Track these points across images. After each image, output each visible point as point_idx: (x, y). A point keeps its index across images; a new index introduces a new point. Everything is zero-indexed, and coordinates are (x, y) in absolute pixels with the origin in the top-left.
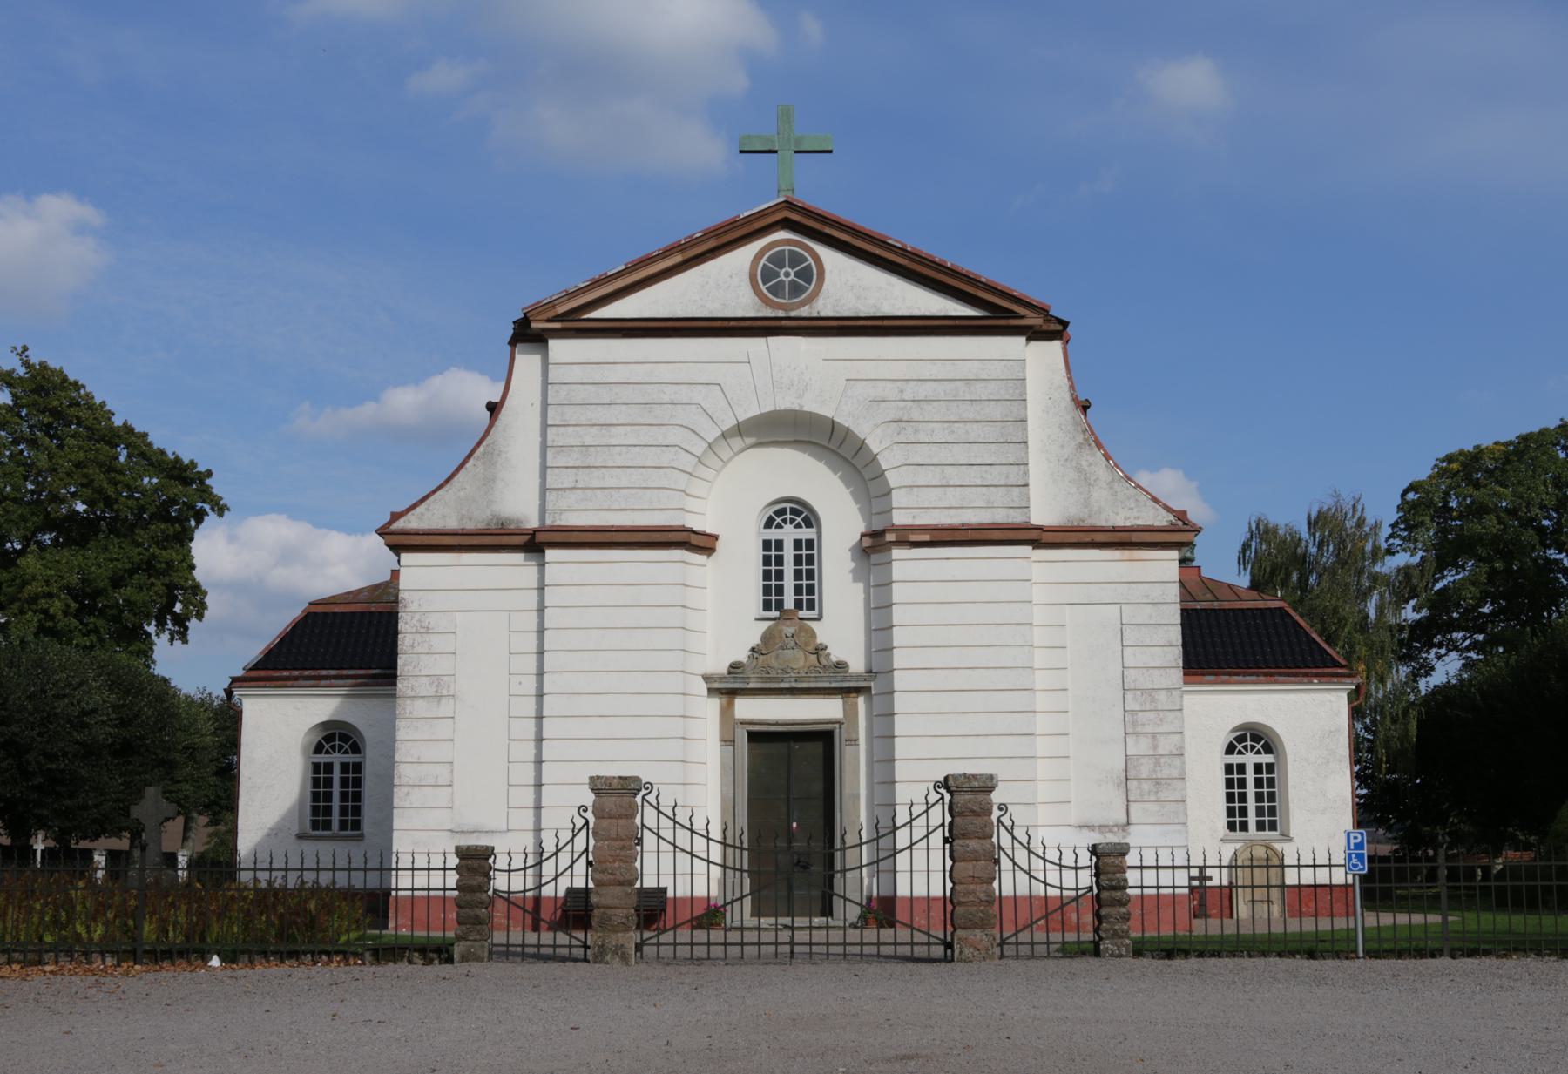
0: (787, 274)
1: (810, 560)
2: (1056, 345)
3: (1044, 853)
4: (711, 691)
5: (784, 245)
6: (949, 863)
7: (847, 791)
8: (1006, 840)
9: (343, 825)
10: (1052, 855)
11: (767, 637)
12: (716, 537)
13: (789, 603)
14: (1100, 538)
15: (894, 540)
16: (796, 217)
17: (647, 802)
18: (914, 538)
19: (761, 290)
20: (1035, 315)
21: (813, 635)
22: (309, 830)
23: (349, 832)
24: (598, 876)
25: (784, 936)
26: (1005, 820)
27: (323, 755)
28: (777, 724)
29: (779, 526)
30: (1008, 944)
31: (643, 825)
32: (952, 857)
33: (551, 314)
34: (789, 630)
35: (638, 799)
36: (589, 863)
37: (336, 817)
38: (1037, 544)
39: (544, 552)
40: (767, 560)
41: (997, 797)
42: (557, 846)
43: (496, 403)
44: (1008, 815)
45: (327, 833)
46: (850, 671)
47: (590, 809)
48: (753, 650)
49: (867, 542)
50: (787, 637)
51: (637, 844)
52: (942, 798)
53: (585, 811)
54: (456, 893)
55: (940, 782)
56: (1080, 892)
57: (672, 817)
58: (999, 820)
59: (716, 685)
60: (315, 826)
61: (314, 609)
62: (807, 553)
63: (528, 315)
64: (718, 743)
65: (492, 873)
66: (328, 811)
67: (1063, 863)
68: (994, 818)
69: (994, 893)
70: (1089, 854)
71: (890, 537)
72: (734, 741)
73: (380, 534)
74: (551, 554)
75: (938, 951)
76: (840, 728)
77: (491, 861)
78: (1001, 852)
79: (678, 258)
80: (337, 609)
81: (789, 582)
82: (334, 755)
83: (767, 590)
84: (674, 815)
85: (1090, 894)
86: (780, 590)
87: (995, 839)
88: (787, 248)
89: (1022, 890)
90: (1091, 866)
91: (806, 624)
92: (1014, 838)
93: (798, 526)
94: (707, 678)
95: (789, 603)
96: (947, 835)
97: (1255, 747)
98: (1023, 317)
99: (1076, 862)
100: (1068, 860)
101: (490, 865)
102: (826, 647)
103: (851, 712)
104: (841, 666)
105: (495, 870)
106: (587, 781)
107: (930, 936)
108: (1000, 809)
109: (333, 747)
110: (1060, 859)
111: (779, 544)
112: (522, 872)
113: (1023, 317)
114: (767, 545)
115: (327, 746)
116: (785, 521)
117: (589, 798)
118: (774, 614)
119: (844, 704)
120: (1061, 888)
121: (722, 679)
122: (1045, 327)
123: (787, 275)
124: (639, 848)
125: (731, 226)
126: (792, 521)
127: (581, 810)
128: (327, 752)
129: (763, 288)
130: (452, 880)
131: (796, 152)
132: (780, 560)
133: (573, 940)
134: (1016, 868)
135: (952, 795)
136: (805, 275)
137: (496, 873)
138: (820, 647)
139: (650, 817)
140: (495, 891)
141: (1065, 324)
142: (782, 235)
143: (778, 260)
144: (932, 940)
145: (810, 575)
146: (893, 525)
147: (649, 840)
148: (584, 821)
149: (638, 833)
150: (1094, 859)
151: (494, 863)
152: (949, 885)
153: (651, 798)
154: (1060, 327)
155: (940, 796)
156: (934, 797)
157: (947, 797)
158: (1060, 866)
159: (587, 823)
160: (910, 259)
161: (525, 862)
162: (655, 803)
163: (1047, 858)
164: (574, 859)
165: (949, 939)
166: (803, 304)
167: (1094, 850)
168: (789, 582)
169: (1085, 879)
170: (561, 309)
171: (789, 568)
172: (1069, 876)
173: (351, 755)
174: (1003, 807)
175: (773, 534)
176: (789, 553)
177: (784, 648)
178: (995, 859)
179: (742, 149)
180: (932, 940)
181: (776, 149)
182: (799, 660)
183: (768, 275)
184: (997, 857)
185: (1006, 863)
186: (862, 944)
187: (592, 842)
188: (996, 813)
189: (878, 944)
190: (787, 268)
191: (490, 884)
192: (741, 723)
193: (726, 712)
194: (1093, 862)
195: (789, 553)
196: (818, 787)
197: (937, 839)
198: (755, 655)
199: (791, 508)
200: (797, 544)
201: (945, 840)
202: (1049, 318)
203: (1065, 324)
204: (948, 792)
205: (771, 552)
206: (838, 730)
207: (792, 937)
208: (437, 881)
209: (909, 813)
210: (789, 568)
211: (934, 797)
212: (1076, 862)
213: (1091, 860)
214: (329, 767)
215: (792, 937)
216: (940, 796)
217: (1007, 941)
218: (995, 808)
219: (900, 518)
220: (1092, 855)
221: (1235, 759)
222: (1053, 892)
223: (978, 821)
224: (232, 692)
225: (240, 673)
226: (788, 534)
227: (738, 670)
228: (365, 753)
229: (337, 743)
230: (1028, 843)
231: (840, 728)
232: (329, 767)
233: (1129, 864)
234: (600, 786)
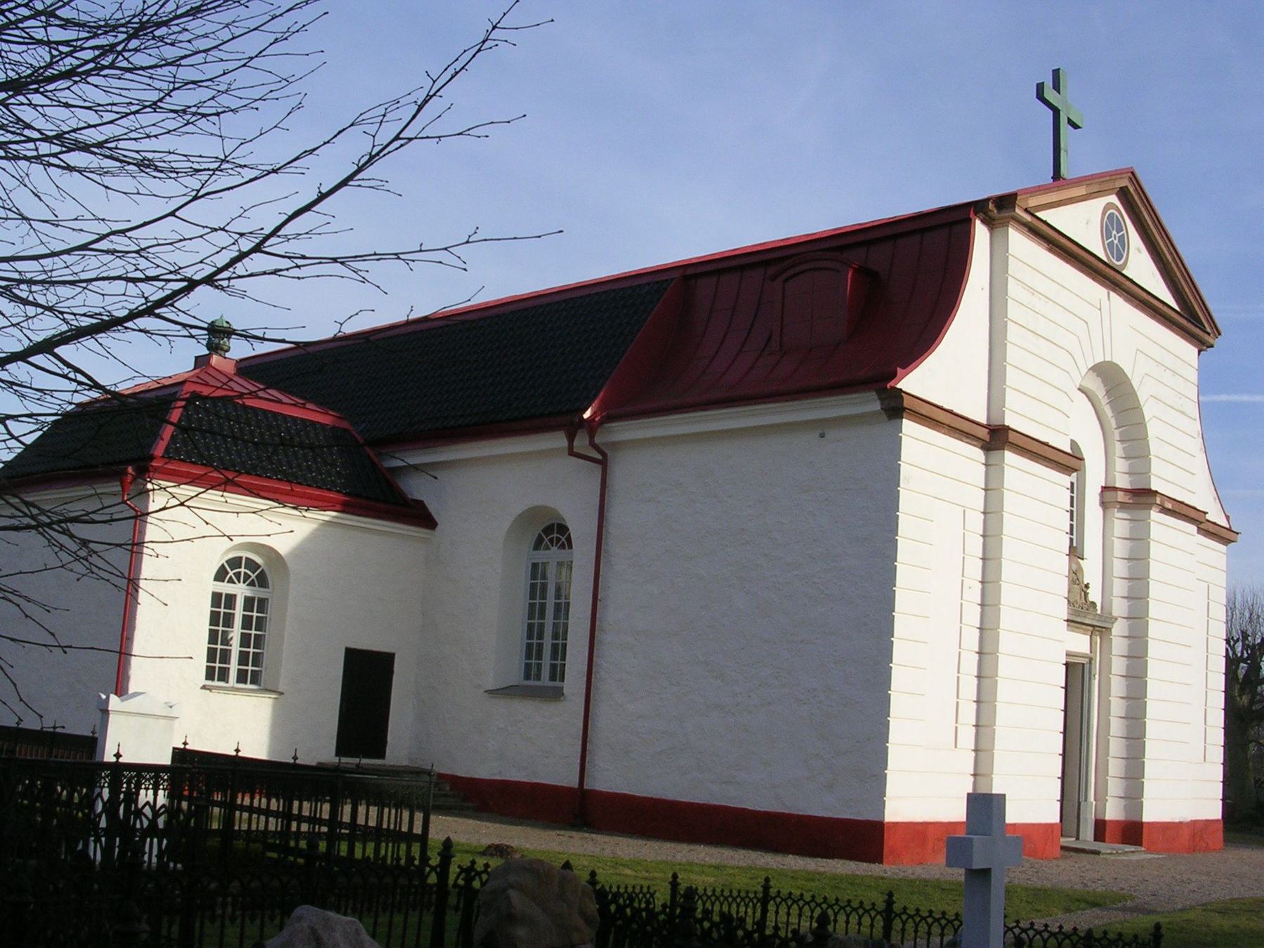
9: (242, 677)
23: (216, 683)
27: (225, 584)
37: (234, 666)
45: (222, 684)
48: (1087, 586)
60: (210, 674)
66: (225, 657)
97: (240, 573)
109: (238, 575)
113: (1209, 334)
125: (1108, 178)
128: (231, 581)
146: (1150, 490)
160: (1174, 259)
173: (257, 588)
214: (231, 599)
229: (243, 570)
231: (1090, 663)
232: (231, 599)
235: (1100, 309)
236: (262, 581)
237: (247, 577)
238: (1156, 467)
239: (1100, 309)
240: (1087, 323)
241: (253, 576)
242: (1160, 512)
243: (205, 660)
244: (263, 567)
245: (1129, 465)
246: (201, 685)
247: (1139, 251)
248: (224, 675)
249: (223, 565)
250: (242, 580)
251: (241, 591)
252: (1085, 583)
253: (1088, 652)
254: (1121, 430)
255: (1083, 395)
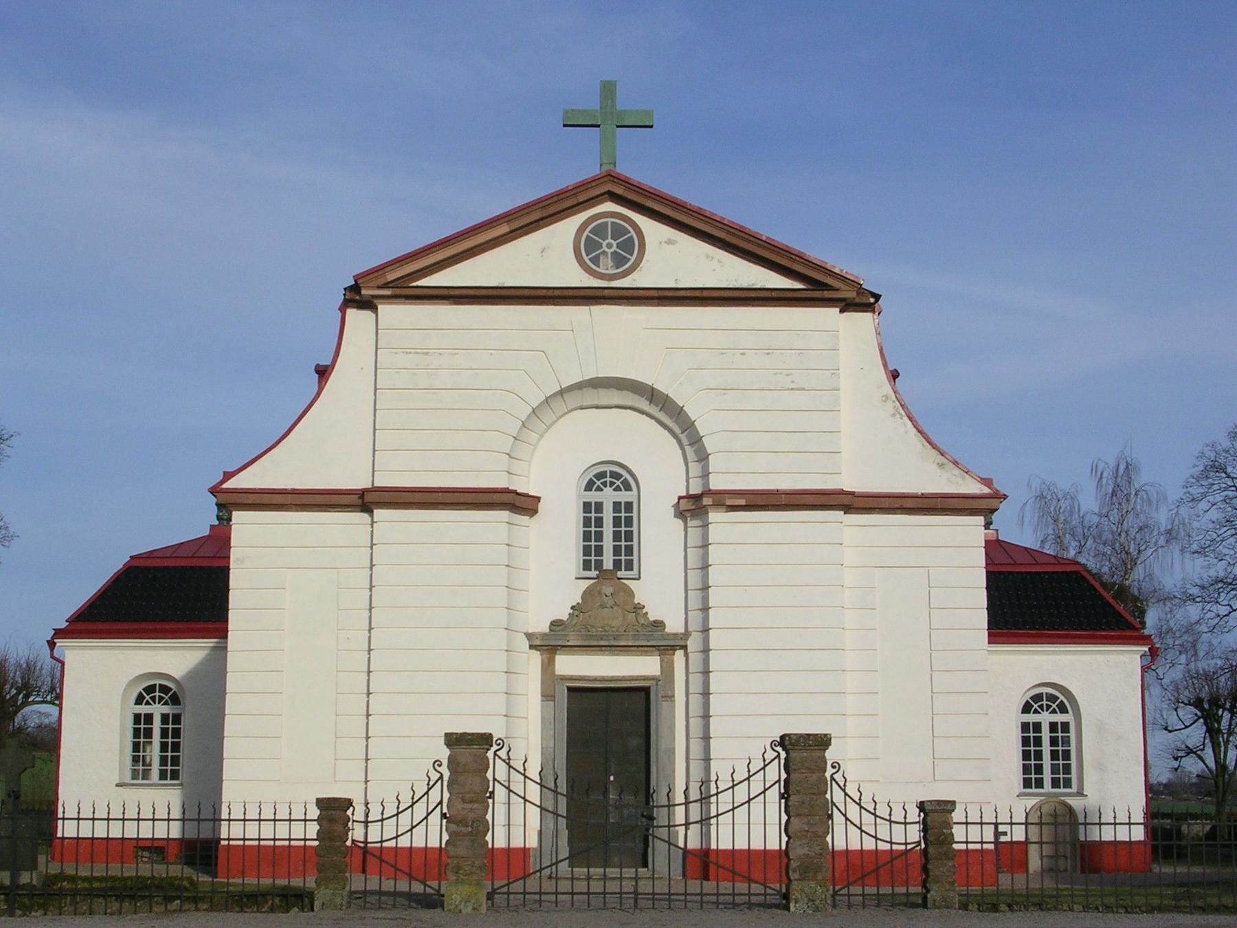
0: (610, 246)
1: (629, 522)
2: (866, 317)
3: (875, 809)
4: (531, 647)
5: (607, 217)
6: (784, 818)
7: (663, 746)
8: (838, 796)
9: (163, 775)
10: (882, 811)
11: (587, 594)
12: (538, 499)
13: (608, 564)
14: (909, 503)
15: (711, 504)
16: (619, 191)
17: (499, 757)
18: (729, 502)
19: (584, 261)
20: (848, 288)
21: (631, 594)
22: (128, 779)
24: (453, 827)
25: (628, 886)
26: (838, 777)
27: (143, 706)
28: (596, 679)
29: (599, 489)
30: (842, 895)
31: (495, 779)
32: (787, 812)
33: (381, 281)
34: (608, 590)
35: (490, 754)
36: (444, 816)
38: (848, 509)
39: (372, 512)
40: (587, 522)
41: (831, 755)
42: (413, 798)
43: (327, 366)
44: (841, 772)
46: (667, 630)
47: (445, 762)
48: (573, 608)
49: (685, 505)
50: (606, 596)
51: (490, 797)
52: (779, 756)
53: (440, 766)
54: (316, 843)
55: (777, 741)
56: (909, 847)
57: (523, 772)
58: (832, 778)
59: (537, 642)
61: (136, 563)
62: (626, 516)
63: (359, 282)
64: (539, 698)
65: (350, 823)
67: (893, 819)
68: (828, 775)
69: (828, 847)
70: (918, 810)
71: (707, 501)
72: (554, 697)
73: (212, 493)
74: (379, 513)
75: (776, 900)
76: (657, 685)
77: (349, 812)
78: (834, 808)
79: (504, 229)
80: (158, 563)
81: (608, 543)
82: (155, 706)
83: (586, 550)
84: (525, 770)
85: (918, 848)
86: (599, 551)
87: (828, 796)
88: (609, 220)
89: (855, 845)
90: (919, 822)
91: (624, 583)
92: (846, 794)
93: (618, 489)
94: (529, 636)
95: (608, 564)
96: (782, 791)
98: (838, 290)
99: (905, 818)
100: (898, 816)
101: (348, 816)
102: (644, 607)
103: (667, 669)
104: (659, 625)
105: (354, 821)
106: (443, 735)
107: (766, 887)
108: (833, 767)
109: (153, 699)
110: (890, 815)
111: (599, 507)
112: (380, 823)
113: (838, 290)
114: (587, 506)
115: (148, 698)
116: (605, 484)
117: (444, 753)
118: (594, 573)
119: (662, 661)
120: (891, 843)
121: (545, 635)
122: (857, 300)
123: (609, 245)
124: (490, 801)
125: (556, 199)
126: (612, 484)
127: (436, 764)
128: (148, 703)
129: (586, 259)
130: (313, 830)
131: (618, 126)
132: (599, 523)
133: (427, 888)
134: (848, 822)
135: (787, 753)
136: (627, 246)
137: (355, 823)
138: (639, 606)
139: (501, 770)
140: (353, 841)
141: (877, 297)
142: (609, 206)
143: (600, 231)
144: (769, 891)
145: (629, 535)
146: (710, 490)
147: (500, 793)
148: (439, 775)
149: (489, 787)
150: (922, 814)
151: (353, 814)
152: (785, 839)
153: (502, 753)
154: (872, 300)
155: (776, 754)
156: (770, 755)
157: (783, 755)
158: (891, 821)
159: (441, 778)
160: (729, 232)
161: (382, 814)
162: (504, 757)
163: (878, 814)
164: (430, 810)
165: (784, 890)
166: (624, 275)
167: (922, 806)
168: (608, 543)
169: (914, 834)
170: (391, 276)
171: (608, 530)
172: (898, 830)
174: (836, 766)
175: (593, 496)
176: (608, 515)
177: (603, 606)
178: (828, 814)
179: (565, 123)
180: (769, 891)
181: (599, 123)
182: (614, 619)
183: (592, 246)
184: (830, 812)
185: (838, 817)
186: (718, 894)
187: (446, 795)
188: (829, 771)
189: (734, 894)
190: (609, 240)
191: (348, 835)
192: (561, 679)
193: (548, 666)
194: (922, 818)
195: (608, 515)
196: (635, 742)
197: (773, 795)
198: (576, 613)
199: (610, 471)
200: (617, 506)
201: (782, 796)
202: (862, 291)
203: (877, 297)
204: (783, 750)
205: (591, 511)
206: (655, 687)
207: (636, 887)
208: (298, 831)
209: (747, 770)
210: (608, 530)
211: (770, 755)
212: (905, 818)
213: (919, 816)
214: (149, 718)
215: (636, 887)
216: (776, 754)
217: (838, 893)
218: (829, 766)
219: (716, 484)
220: (920, 812)
221: (1031, 718)
222: (883, 846)
223: (815, 777)
224: (55, 644)
225: (63, 625)
226: (608, 497)
227: (561, 628)
228: (184, 703)
229: (157, 694)
230: (860, 799)
231: (657, 685)
232: (149, 718)
233: (954, 821)
234: (453, 740)
235: (573, 331)
236: (175, 700)
237: (1048, 707)
238: (714, 463)
239: (573, 331)
240: (543, 352)
241: (167, 697)
242: (727, 512)
243: (158, 765)
244: (174, 689)
245: (702, 467)
246: (115, 784)
247: (670, 242)
248: (146, 775)
249: (141, 693)
250: (157, 702)
251: (157, 710)
252: (636, 602)
253: (659, 674)
254: (686, 433)
255: (628, 410)
